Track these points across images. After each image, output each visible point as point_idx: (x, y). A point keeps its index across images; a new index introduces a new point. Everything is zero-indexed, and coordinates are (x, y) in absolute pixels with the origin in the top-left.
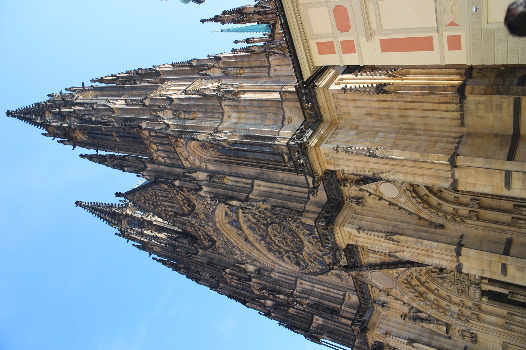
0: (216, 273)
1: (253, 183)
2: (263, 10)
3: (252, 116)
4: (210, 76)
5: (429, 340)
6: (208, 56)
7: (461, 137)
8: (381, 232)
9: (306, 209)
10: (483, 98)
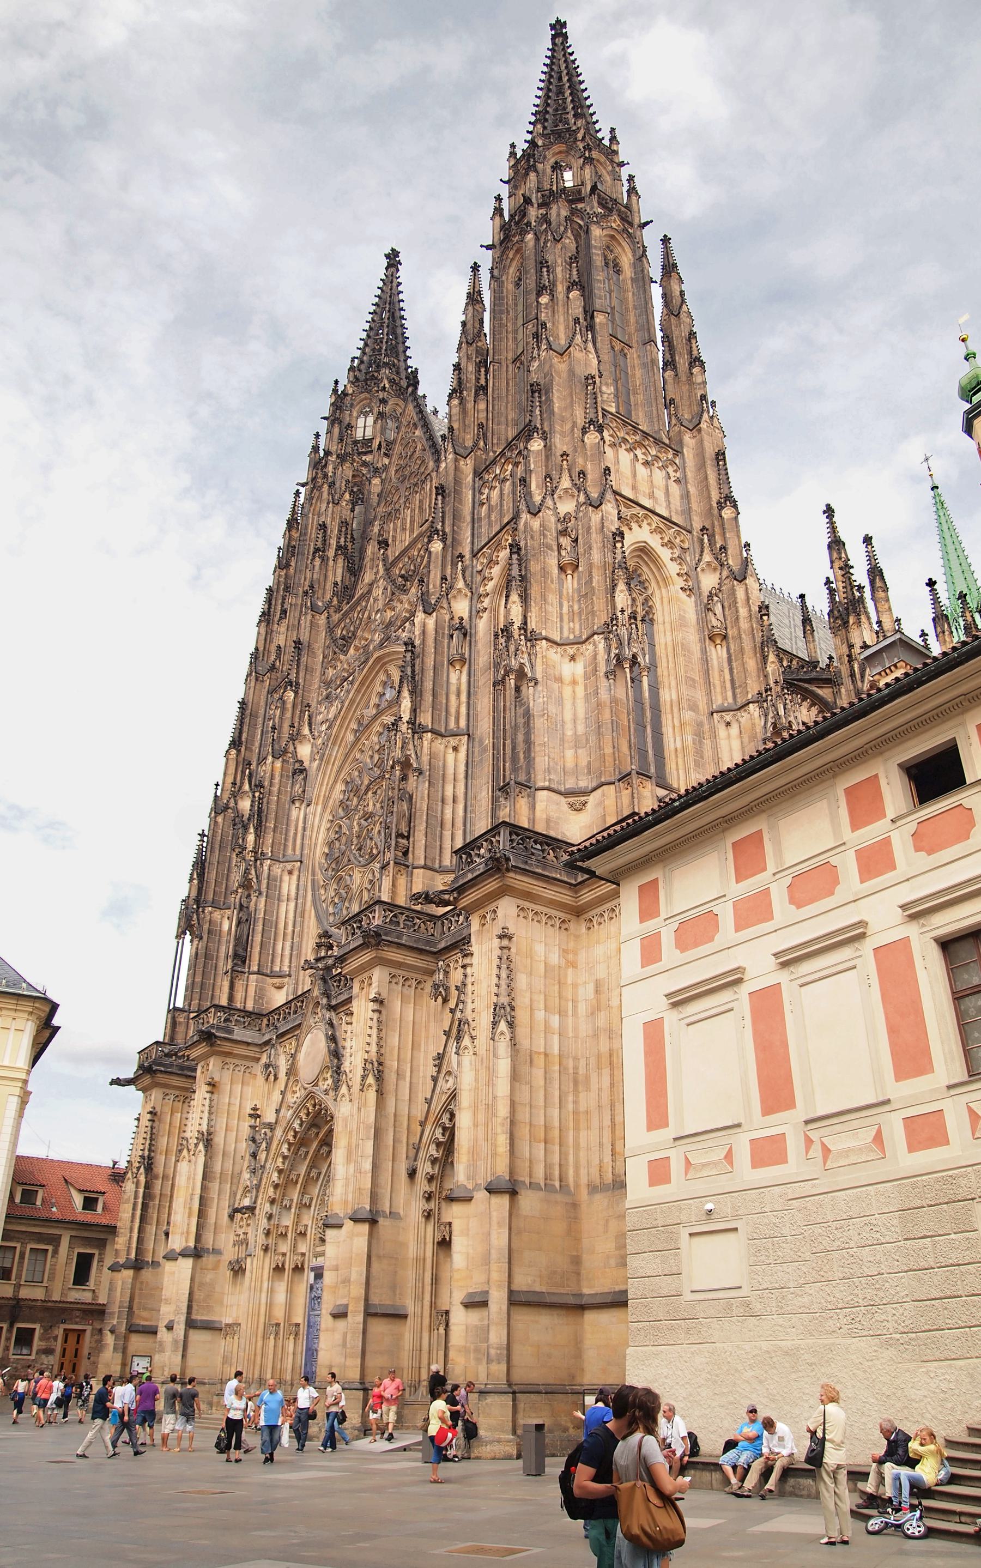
3: (581, 713)
4: (699, 560)
5: (218, 1176)
6: (747, 545)
8: (379, 1046)
9: (415, 871)
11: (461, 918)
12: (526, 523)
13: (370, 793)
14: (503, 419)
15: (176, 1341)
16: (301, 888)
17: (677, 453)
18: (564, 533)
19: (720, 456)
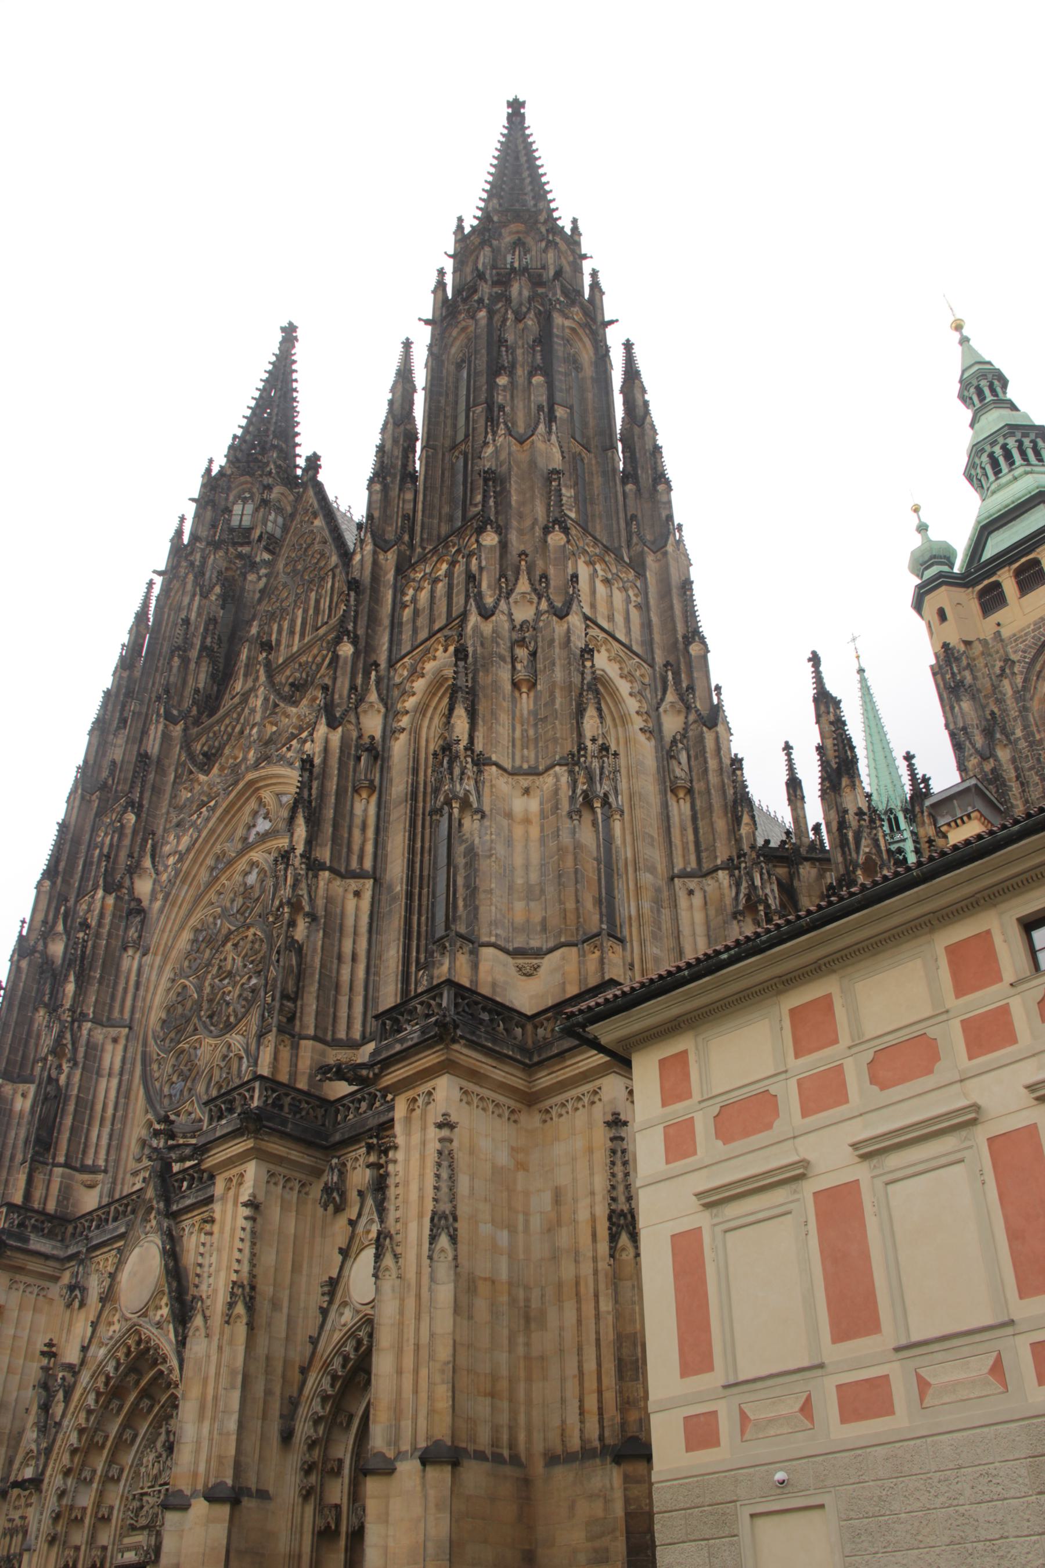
0: (125, 779)
1: (361, 875)
2: (850, 835)
3: (535, 858)
4: (662, 700)
7: (515, 1460)
9: (303, 1042)
10: (619, 1509)
11: (364, 1105)
12: (476, 628)
13: (229, 944)
14: (436, 513)
16: (129, 1061)
17: (641, 574)
18: (521, 642)
19: (687, 585)
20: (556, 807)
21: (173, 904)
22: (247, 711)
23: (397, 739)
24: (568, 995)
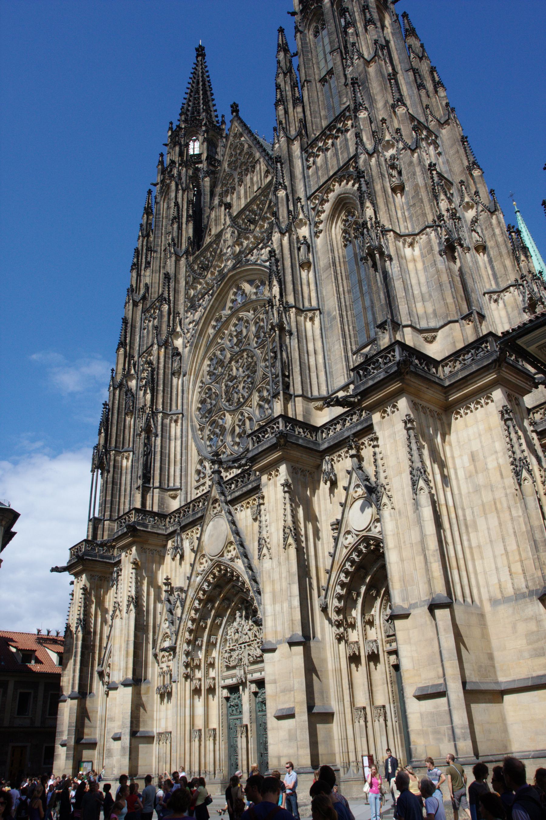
0: (155, 292)
3: (423, 279)
9: (297, 399)
11: (339, 427)
14: (318, 115)
15: (123, 748)
20: (431, 249)
21: (196, 347)
22: (222, 241)
23: (318, 237)
24: (458, 348)
